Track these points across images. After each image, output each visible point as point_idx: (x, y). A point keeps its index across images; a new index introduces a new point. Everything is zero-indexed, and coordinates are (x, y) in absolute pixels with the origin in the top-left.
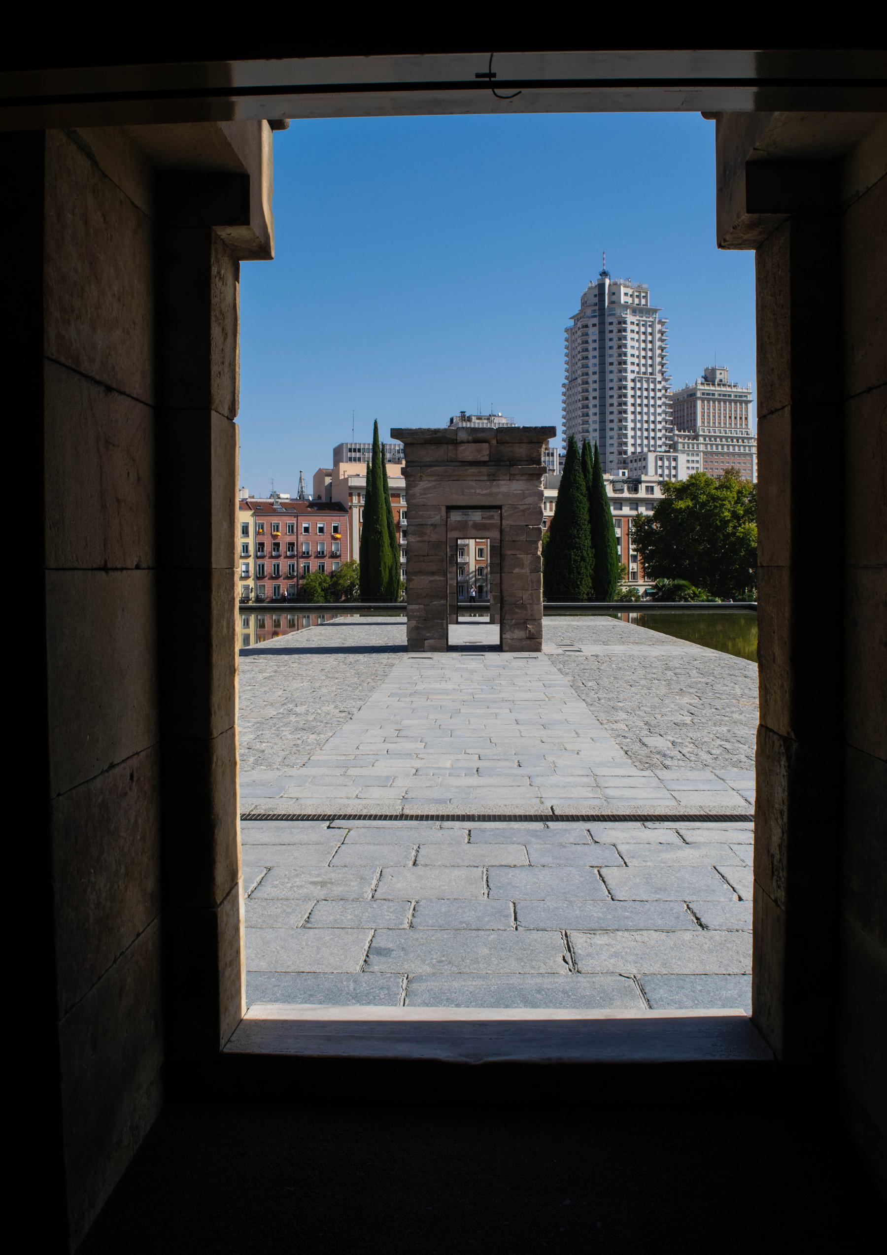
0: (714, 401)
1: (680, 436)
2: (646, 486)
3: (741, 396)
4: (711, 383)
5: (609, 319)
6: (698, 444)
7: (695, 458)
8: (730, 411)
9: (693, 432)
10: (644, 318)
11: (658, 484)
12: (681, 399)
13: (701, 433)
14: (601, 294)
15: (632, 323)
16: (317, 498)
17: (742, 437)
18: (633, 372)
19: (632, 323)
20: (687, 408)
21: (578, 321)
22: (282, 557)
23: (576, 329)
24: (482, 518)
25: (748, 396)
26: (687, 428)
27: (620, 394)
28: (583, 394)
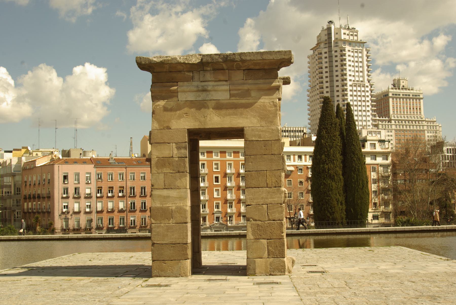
0: (400, 98)
1: (381, 121)
2: (370, 143)
3: (416, 96)
4: (397, 88)
5: (334, 49)
6: (391, 125)
7: (390, 134)
8: (410, 104)
9: (388, 118)
10: (356, 48)
11: (379, 142)
12: (380, 98)
13: (393, 118)
14: (329, 34)
15: (349, 51)
16: (142, 156)
17: (418, 120)
18: (350, 80)
19: (349, 51)
20: (384, 103)
21: (316, 50)
22: (116, 197)
23: (315, 56)
24: (231, 96)
25: (421, 95)
26: (384, 115)
27: (343, 94)
28: (320, 95)
